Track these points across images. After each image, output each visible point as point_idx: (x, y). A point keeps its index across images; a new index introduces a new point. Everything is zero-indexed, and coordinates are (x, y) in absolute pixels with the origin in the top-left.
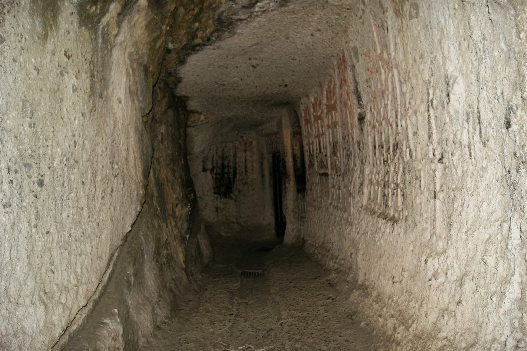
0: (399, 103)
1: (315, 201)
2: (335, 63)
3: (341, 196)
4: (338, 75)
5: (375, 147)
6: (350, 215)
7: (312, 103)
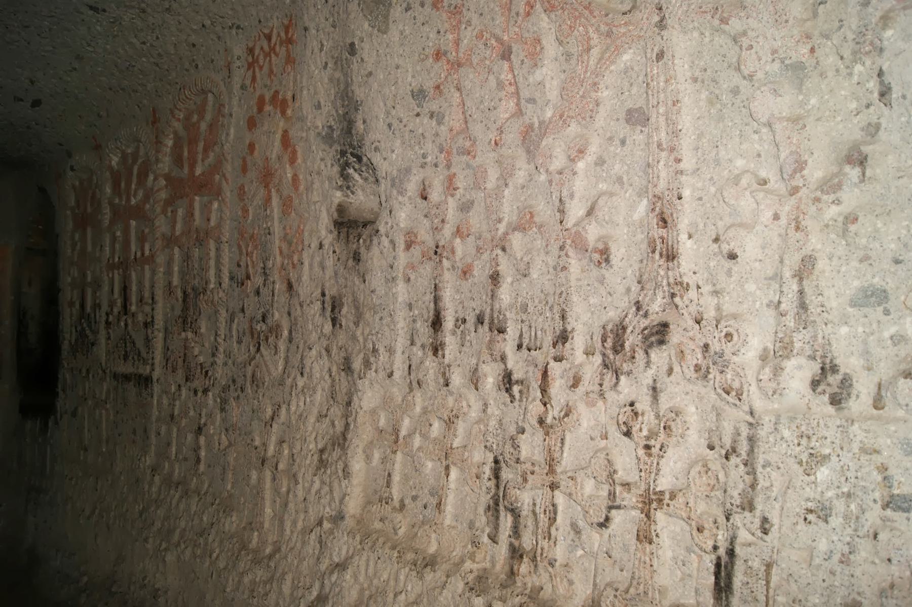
0: (687, 164)
1: (86, 450)
2: (239, 50)
3: (203, 454)
4: (243, 87)
5: (437, 323)
6: (252, 525)
7: (110, 168)
